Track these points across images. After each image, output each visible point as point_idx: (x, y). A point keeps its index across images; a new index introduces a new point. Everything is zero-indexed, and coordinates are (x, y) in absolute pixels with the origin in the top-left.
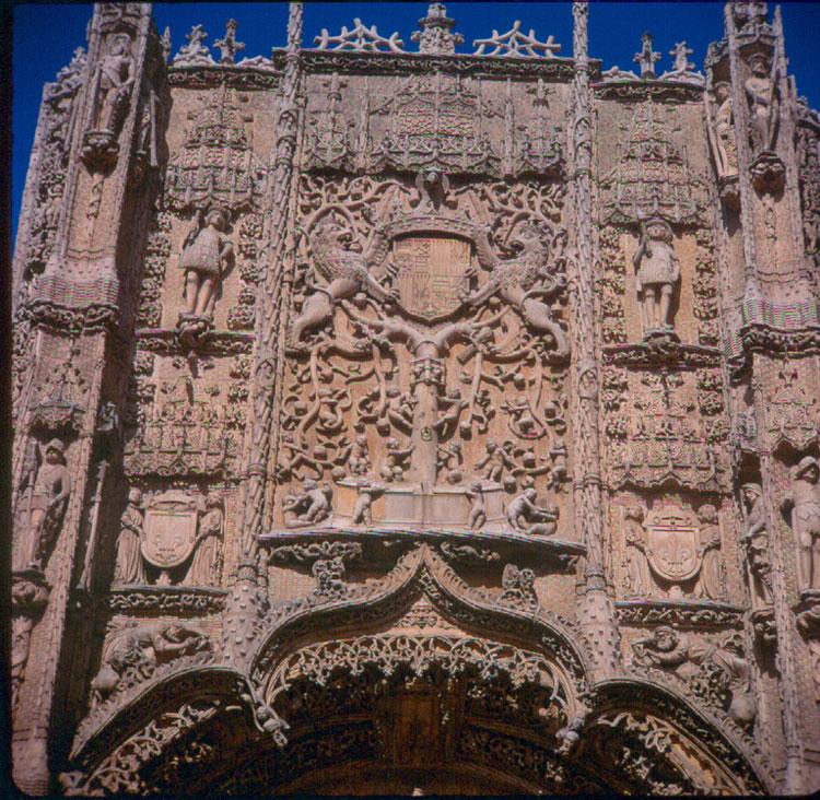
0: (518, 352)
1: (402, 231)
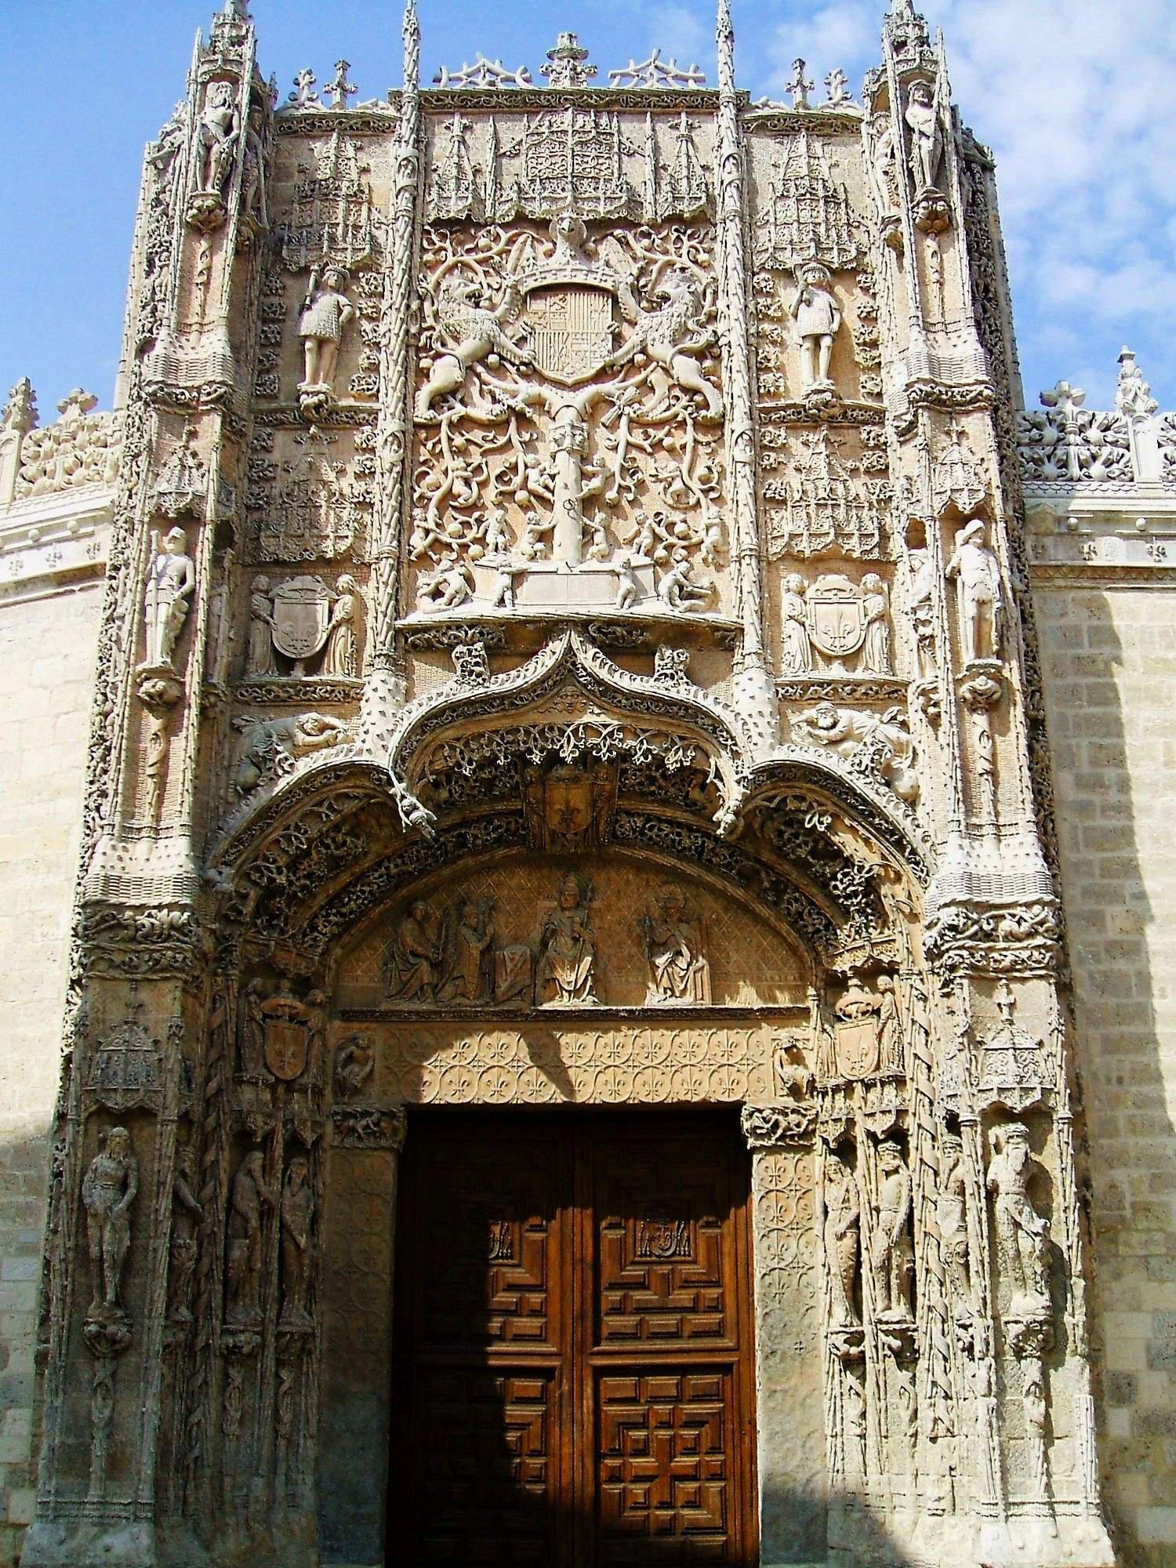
1: (537, 284)
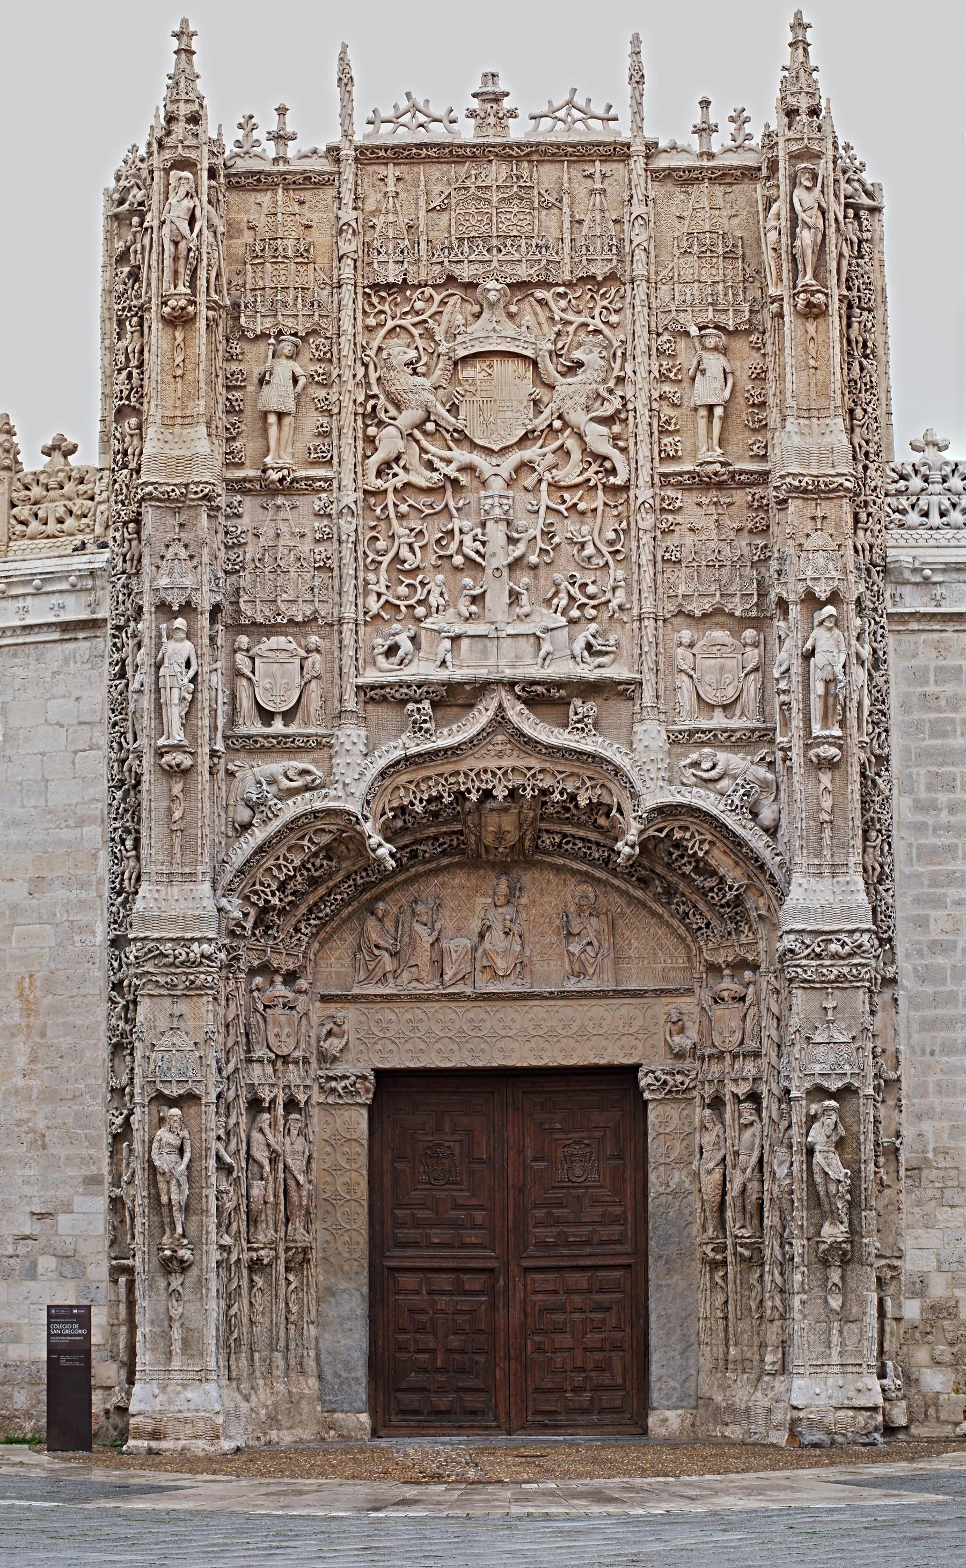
0: (581, 479)
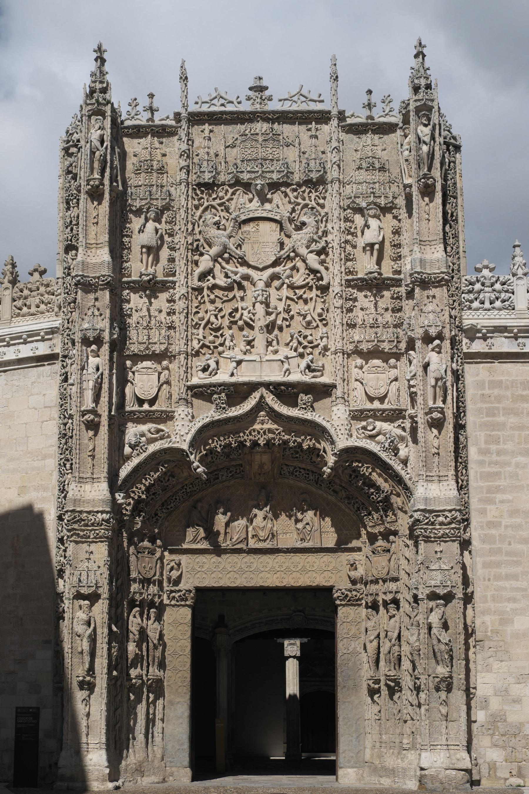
0: (304, 282)
